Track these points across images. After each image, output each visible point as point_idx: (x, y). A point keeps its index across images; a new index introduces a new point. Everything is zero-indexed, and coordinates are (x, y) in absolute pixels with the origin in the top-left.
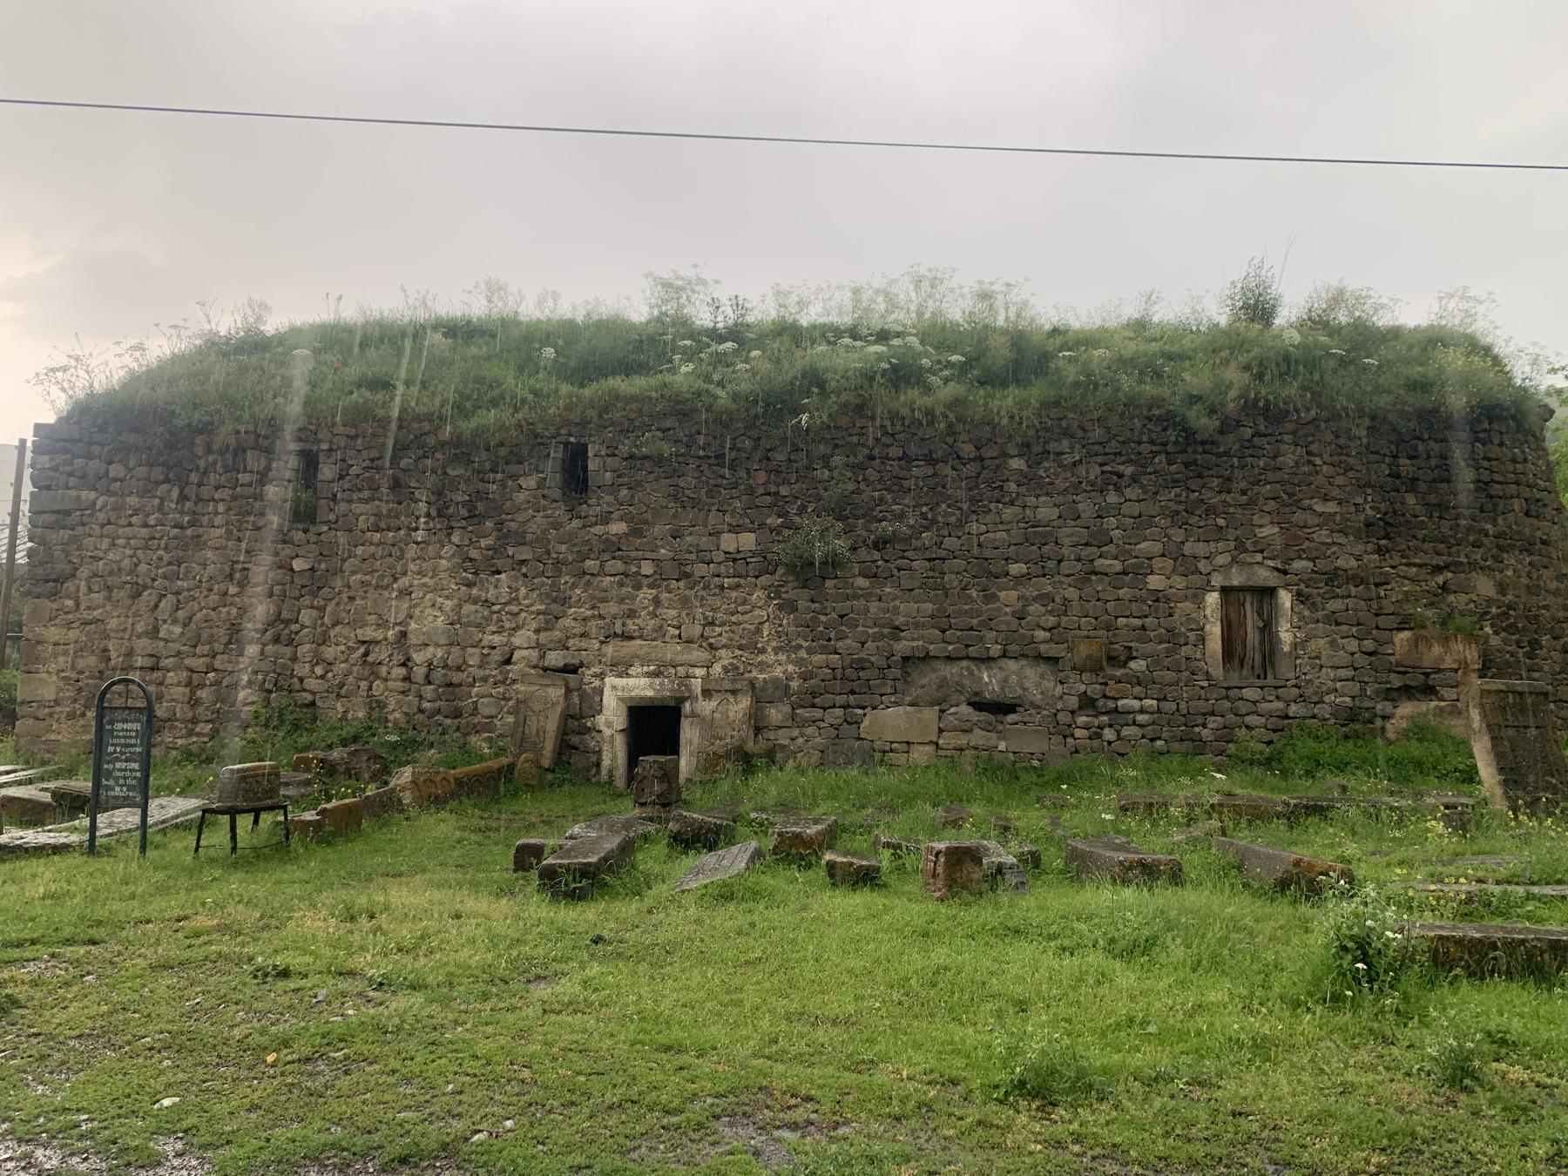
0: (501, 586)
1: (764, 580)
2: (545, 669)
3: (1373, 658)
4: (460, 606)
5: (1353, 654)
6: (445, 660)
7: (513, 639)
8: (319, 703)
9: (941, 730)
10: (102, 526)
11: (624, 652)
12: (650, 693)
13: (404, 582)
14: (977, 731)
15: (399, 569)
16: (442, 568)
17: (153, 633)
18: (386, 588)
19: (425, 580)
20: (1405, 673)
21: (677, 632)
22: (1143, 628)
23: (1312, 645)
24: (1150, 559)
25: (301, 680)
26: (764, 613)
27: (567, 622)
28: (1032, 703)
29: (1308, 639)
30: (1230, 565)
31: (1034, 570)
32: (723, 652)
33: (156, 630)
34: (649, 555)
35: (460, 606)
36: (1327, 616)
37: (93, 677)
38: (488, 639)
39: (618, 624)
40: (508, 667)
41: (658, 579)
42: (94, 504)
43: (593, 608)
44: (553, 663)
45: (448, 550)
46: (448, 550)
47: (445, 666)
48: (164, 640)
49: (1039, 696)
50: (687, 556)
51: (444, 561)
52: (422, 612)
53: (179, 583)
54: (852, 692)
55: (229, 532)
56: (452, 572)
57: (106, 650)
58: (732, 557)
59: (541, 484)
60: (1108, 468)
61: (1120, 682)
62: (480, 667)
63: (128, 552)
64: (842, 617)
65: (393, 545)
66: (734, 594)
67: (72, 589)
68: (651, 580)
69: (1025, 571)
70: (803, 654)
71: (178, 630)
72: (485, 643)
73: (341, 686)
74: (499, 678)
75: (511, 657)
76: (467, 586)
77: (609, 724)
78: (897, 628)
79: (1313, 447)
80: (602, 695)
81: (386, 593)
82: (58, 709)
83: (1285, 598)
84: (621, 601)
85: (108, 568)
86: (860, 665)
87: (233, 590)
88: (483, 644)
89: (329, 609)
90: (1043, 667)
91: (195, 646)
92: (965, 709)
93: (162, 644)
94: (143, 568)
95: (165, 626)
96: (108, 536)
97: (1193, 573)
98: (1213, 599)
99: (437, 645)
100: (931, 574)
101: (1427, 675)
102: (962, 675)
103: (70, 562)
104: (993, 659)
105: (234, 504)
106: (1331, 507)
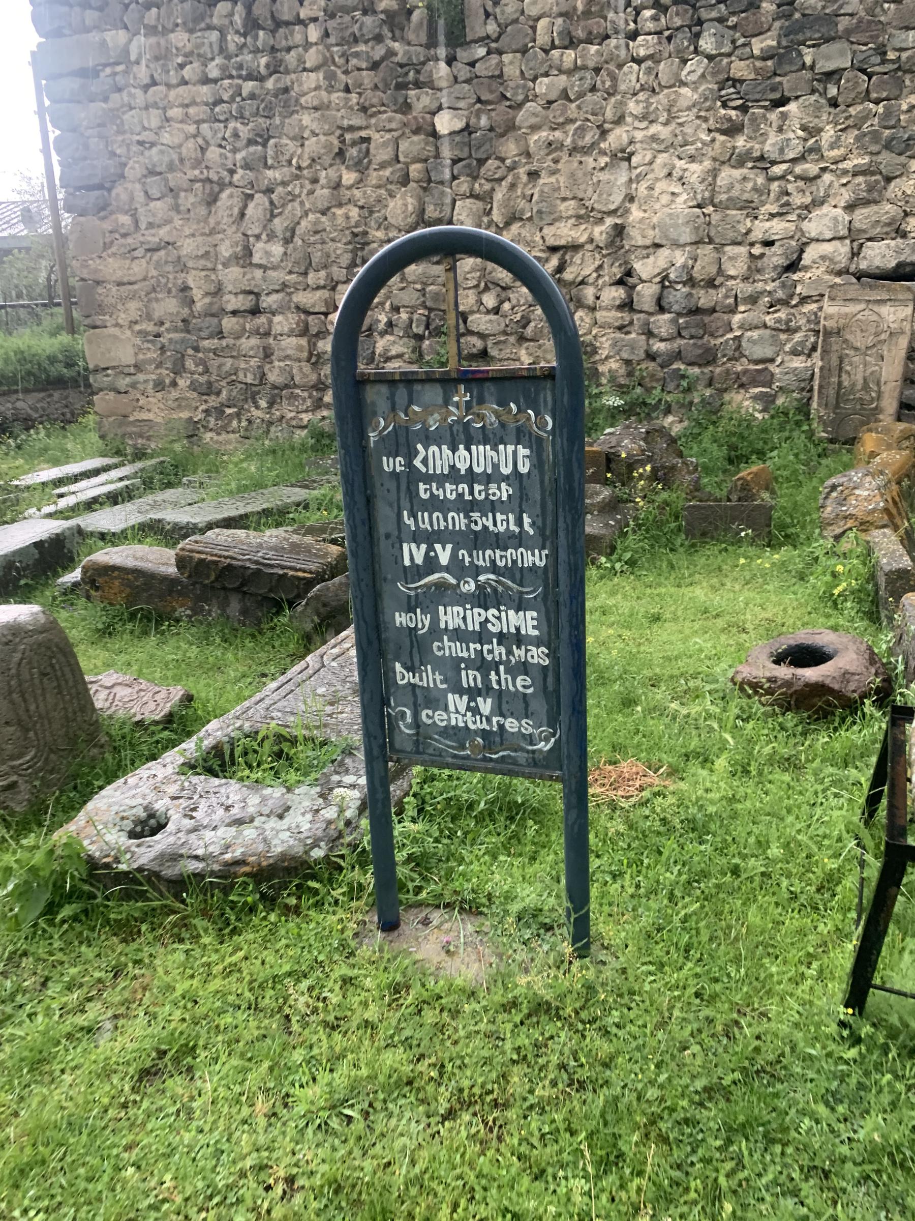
2: (860, 276)
4: (714, 173)
6: (688, 269)
7: (805, 225)
8: (493, 352)
10: (146, 88)
13: (617, 137)
15: (609, 114)
16: (683, 103)
17: (245, 257)
18: (586, 151)
19: (655, 129)
33: (248, 252)
35: (714, 173)
37: (176, 330)
38: (761, 229)
40: (795, 277)
42: (126, 51)
44: (878, 262)
45: (695, 67)
46: (695, 67)
47: (691, 281)
48: (260, 266)
51: (684, 91)
52: (651, 188)
53: (270, 173)
55: (330, 77)
56: (702, 113)
57: (185, 288)
62: (745, 279)
63: (192, 129)
65: (597, 70)
67: (124, 197)
72: (757, 235)
74: (780, 294)
75: (800, 258)
76: (724, 132)
81: (589, 161)
82: (141, 377)
85: (166, 159)
87: (349, 177)
88: (753, 237)
89: (499, 196)
91: (305, 274)
93: (258, 273)
94: (213, 153)
95: (260, 245)
96: (155, 105)
99: (676, 245)
103: (113, 154)
105: (331, 24)
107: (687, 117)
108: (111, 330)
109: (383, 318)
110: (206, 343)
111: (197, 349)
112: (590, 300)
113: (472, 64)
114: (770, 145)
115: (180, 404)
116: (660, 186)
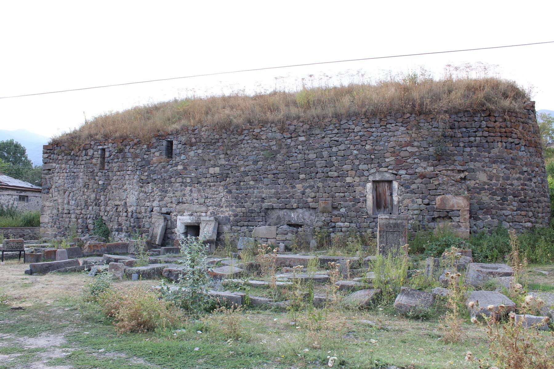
1: (223, 183)
2: (162, 213)
3: (427, 206)
5: (420, 205)
9: (277, 234)
10: (58, 173)
12: (190, 221)
13: (125, 187)
14: (290, 234)
17: (68, 203)
18: (121, 189)
19: (131, 186)
22: (344, 196)
23: (405, 202)
24: (348, 171)
26: (223, 194)
27: (166, 198)
28: (307, 224)
29: (404, 199)
30: (375, 173)
31: (308, 177)
32: (210, 208)
34: (189, 176)
35: (139, 194)
36: (411, 191)
37: (55, 216)
40: (152, 213)
41: (191, 184)
43: (174, 193)
45: (136, 177)
46: (136, 177)
47: (136, 213)
49: (309, 222)
50: (199, 176)
53: (74, 189)
54: (249, 221)
55: (84, 173)
57: (58, 208)
58: (213, 176)
59: (161, 154)
60: (333, 139)
63: (63, 180)
64: (246, 195)
66: (214, 188)
68: (189, 184)
70: (234, 208)
71: (73, 202)
72: (146, 205)
73: (111, 218)
74: (150, 216)
77: (178, 231)
78: (263, 198)
79: (409, 127)
80: (176, 221)
82: (48, 225)
83: (395, 184)
84: (181, 191)
86: (252, 212)
87: (86, 190)
88: (146, 205)
90: (312, 211)
92: (285, 227)
94: (66, 185)
97: (362, 176)
98: (369, 185)
100: (274, 179)
101: (448, 212)
102: (284, 214)
104: (293, 209)
106: (415, 150)
108: (45, 215)
109: (89, 216)
110: (60, 219)
111: (59, 220)
112: (121, 215)
113: (105, 173)
114: (147, 190)
115: (54, 230)
116: (131, 195)
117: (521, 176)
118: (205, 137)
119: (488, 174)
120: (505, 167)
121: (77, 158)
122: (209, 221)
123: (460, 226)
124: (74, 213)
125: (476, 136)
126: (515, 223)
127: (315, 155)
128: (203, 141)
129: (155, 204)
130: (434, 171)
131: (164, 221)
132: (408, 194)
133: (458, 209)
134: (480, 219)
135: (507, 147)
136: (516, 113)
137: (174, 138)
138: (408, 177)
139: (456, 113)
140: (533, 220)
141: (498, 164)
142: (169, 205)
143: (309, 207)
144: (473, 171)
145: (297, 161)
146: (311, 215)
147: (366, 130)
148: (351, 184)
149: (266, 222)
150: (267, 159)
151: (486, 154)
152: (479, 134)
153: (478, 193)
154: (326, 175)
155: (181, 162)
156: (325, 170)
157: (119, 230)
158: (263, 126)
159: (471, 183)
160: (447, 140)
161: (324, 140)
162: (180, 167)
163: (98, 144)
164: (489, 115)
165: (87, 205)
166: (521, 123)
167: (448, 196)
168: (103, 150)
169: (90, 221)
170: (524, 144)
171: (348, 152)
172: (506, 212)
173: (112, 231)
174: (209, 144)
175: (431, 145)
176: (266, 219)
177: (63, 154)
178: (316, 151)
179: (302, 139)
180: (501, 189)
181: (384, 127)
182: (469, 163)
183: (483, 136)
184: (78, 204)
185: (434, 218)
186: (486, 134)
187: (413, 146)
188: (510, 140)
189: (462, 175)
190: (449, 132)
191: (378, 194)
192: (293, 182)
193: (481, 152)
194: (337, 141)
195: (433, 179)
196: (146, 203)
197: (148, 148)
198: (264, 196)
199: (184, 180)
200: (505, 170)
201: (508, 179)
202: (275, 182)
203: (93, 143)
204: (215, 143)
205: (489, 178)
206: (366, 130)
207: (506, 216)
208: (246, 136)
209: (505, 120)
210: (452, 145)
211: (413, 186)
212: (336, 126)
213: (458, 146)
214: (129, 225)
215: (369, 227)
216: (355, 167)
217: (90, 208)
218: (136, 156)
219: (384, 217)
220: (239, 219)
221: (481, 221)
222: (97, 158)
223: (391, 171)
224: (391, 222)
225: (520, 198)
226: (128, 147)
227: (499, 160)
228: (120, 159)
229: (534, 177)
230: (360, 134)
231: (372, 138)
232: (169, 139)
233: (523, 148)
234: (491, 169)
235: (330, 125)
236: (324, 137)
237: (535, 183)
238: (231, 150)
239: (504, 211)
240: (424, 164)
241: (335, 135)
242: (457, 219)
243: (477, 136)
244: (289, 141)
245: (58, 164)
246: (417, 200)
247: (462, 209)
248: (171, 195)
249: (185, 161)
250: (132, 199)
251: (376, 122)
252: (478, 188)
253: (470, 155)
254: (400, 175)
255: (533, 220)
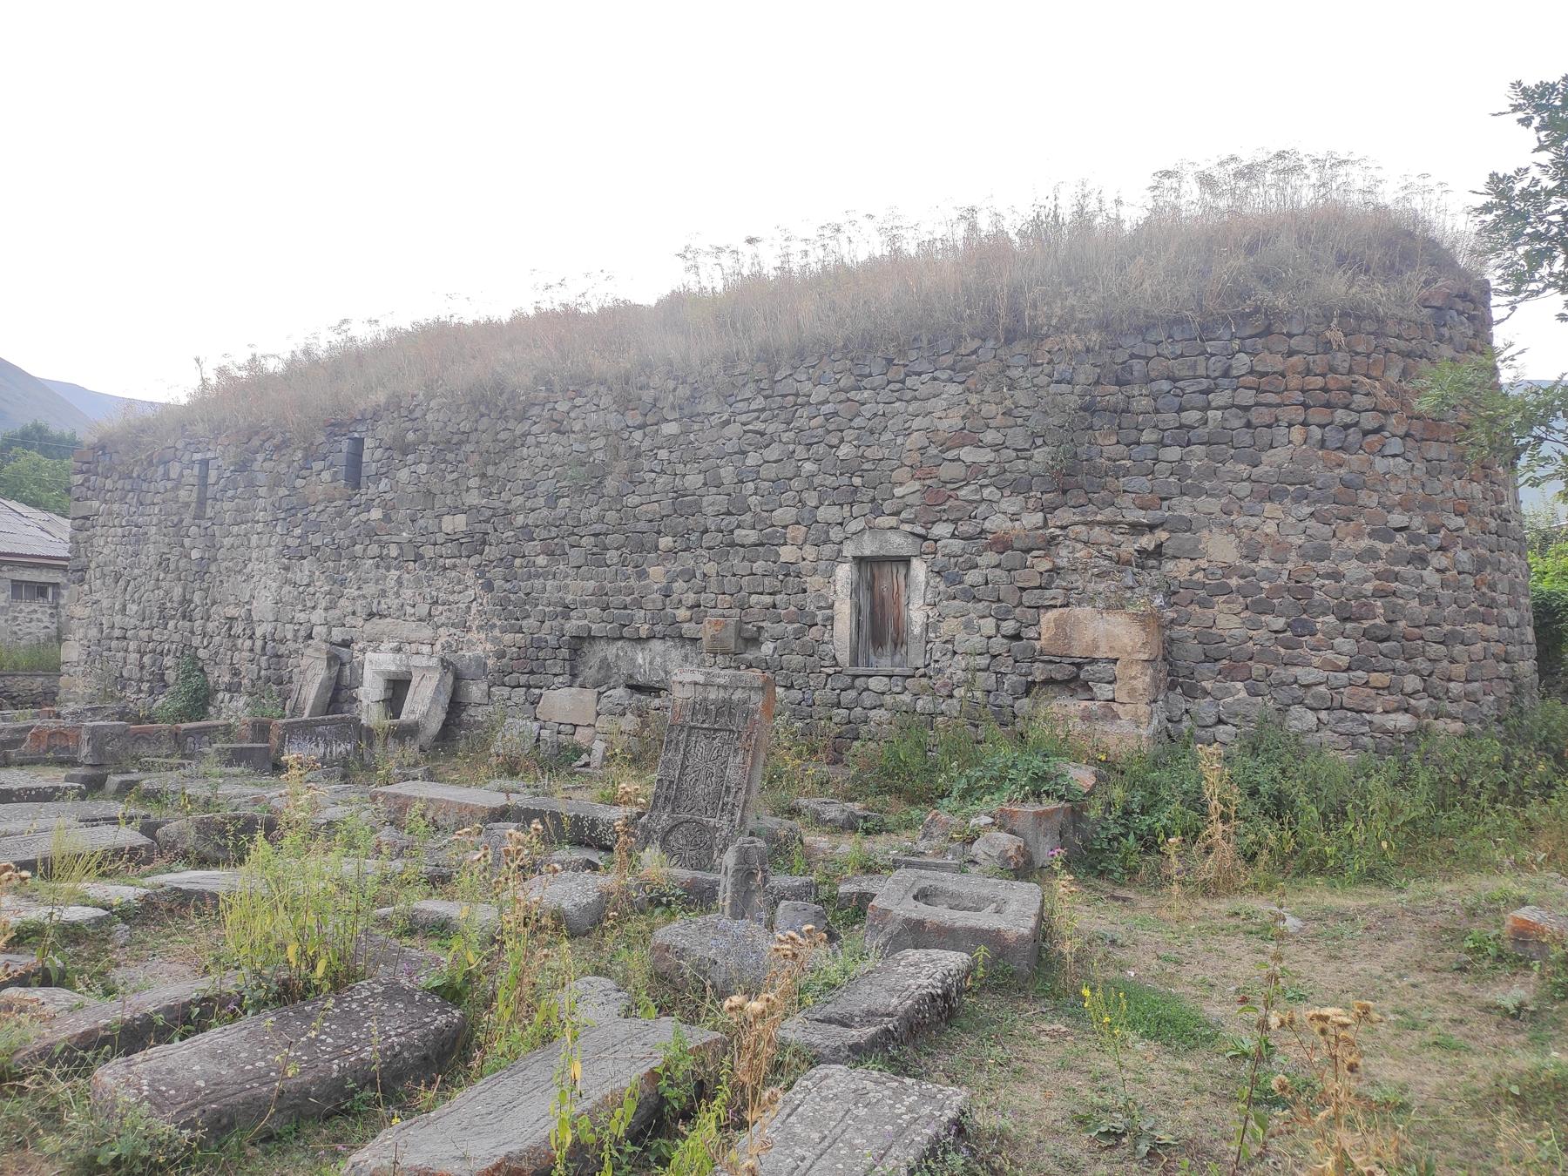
0: (304, 571)
1: (475, 560)
2: (332, 644)
5: (990, 638)
9: (598, 714)
11: (378, 628)
12: (393, 668)
13: (250, 566)
16: (270, 555)
18: (240, 572)
20: (1051, 662)
21: (412, 611)
22: (774, 606)
24: (785, 527)
25: (197, 648)
26: (472, 592)
27: (343, 602)
29: (942, 617)
32: (441, 631)
35: (281, 588)
36: (964, 591)
37: (95, 645)
39: (376, 602)
43: (359, 588)
45: (275, 539)
46: (275, 539)
47: (274, 640)
54: (532, 672)
55: (160, 529)
60: (750, 427)
61: (749, 667)
64: (527, 594)
66: (453, 574)
69: (671, 544)
70: (497, 632)
71: (135, 607)
73: (217, 653)
83: (919, 569)
84: (377, 582)
92: (620, 692)
98: (844, 572)
101: (1079, 666)
102: (617, 655)
104: (639, 640)
106: (984, 456)
107: (271, 561)
117: (1379, 545)
118: (437, 426)
119: (1246, 536)
120: (1312, 514)
121: (145, 486)
122: (428, 668)
123: (1116, 717)
124: (136, 637)
125: (1208, 407)
126: (1340, 713)
127: (702, 476)
128: (431, 438)
129: (317, 616)
130: (1045, 525)
131: (329, 666)
132: (957, 602)
133: (1111, 656)
134: (1206, 693)
135: (1327, 443)
136: (1380, 321)
137: (368, 430)
138: (957, 545)
139: (1142, 331)
140: (1422, 703)
141: (1287, 501)
142: (349, 620)
143: (681, 637)
144: (1188, 524)
145: (654, 498)
146: (686, 661)
147: (843, 396)
148: (792, 568)
149: (574, 676)
150: (581, 490)
151: (1243, 467)
152: (1218, 399)
153: (1204, 604)
154: (727, 539)
155: (378, 500)
156: (725, 522)
157: (234, 689)
158: (579, 394)
159: (1179, 569)
160: (1097, 422)
161: (728, 431)
162: (376, 514)
163: (192, 448)
164: (1267, 332)
165: (164, 618)
166: (1396, 357)
167: (1082, 612)
168: (205, 463)
169: (169, 661)
170: (1402, 431)
171: (789, 470)
172: (1305, 674)
173: (217, 691)
174: (448, 446)
175: (1039, 441)
176: (573, 668)
177: (116, 477)
178: (704, 465)
179: (670, 428)
180: (1288, 590)
181: (899, 386)
182: (1174, 501)
183: (1233, 406)
184: (144, 613)
185: (1034, 682)
186: (1247, 397)
187: (979, 444)
188: (1341, 415)
189: (1147, 541)
190: (1112, 395)
191: (878, 601)
192: (641, 562)
193: (1223, 462)
194: (762, 434)
195: (1035, 553)
196: (298, 615)
197: (305, 458)
198: (569, 598)
199: (385, 552)
200: (1312, 523)
201: (1322, 554)
202: (596, 558)
203: (180, 445)
204: (460, 443)
205: (1245, 552)
206: (843, 396)
207: (1308, 686)
208: (535, 423)
209: (1327, 347)
210: (1114, 439)
211: (972, 577)
212: (762, 386)
213: (1138, 444)
214: (255, 676)
215: (838, 705)
216: (807, 515)
217: (171, 624)
218: (276, 483)
219: (688, 677)
220: (507, 665)
221: (1209, 699)
222: (189, 488)
223: (907, 527)
224: (712, 696)
225: (1366, 624)
226: (260, 457)
227: (1291, 488)
228: (240, 490)
229: (1440, 548)
230: (826, 409)
231: (857, 422)
232: (356, 435)
233: (1395, 446)
234: (1255, 521)
235: (744, 385)
236: (727, 422)
237: (1438, 570)
238: (496, 464)
239: (1298, 671)
240: (1011, 504)
241: (756, 414)
242: (1104, 691)
243: (1213, 404)
244: (638, 435)
245: (105, 502)
246: (982, 621)
247: (1124, 658)
248: (351, 591)
249: (387, 496)
250: (263, 606)
251: (876, 371)
252: (1204, 586)
253: (1180, 469)
254: (936, 541)
255: (1422, 703)
